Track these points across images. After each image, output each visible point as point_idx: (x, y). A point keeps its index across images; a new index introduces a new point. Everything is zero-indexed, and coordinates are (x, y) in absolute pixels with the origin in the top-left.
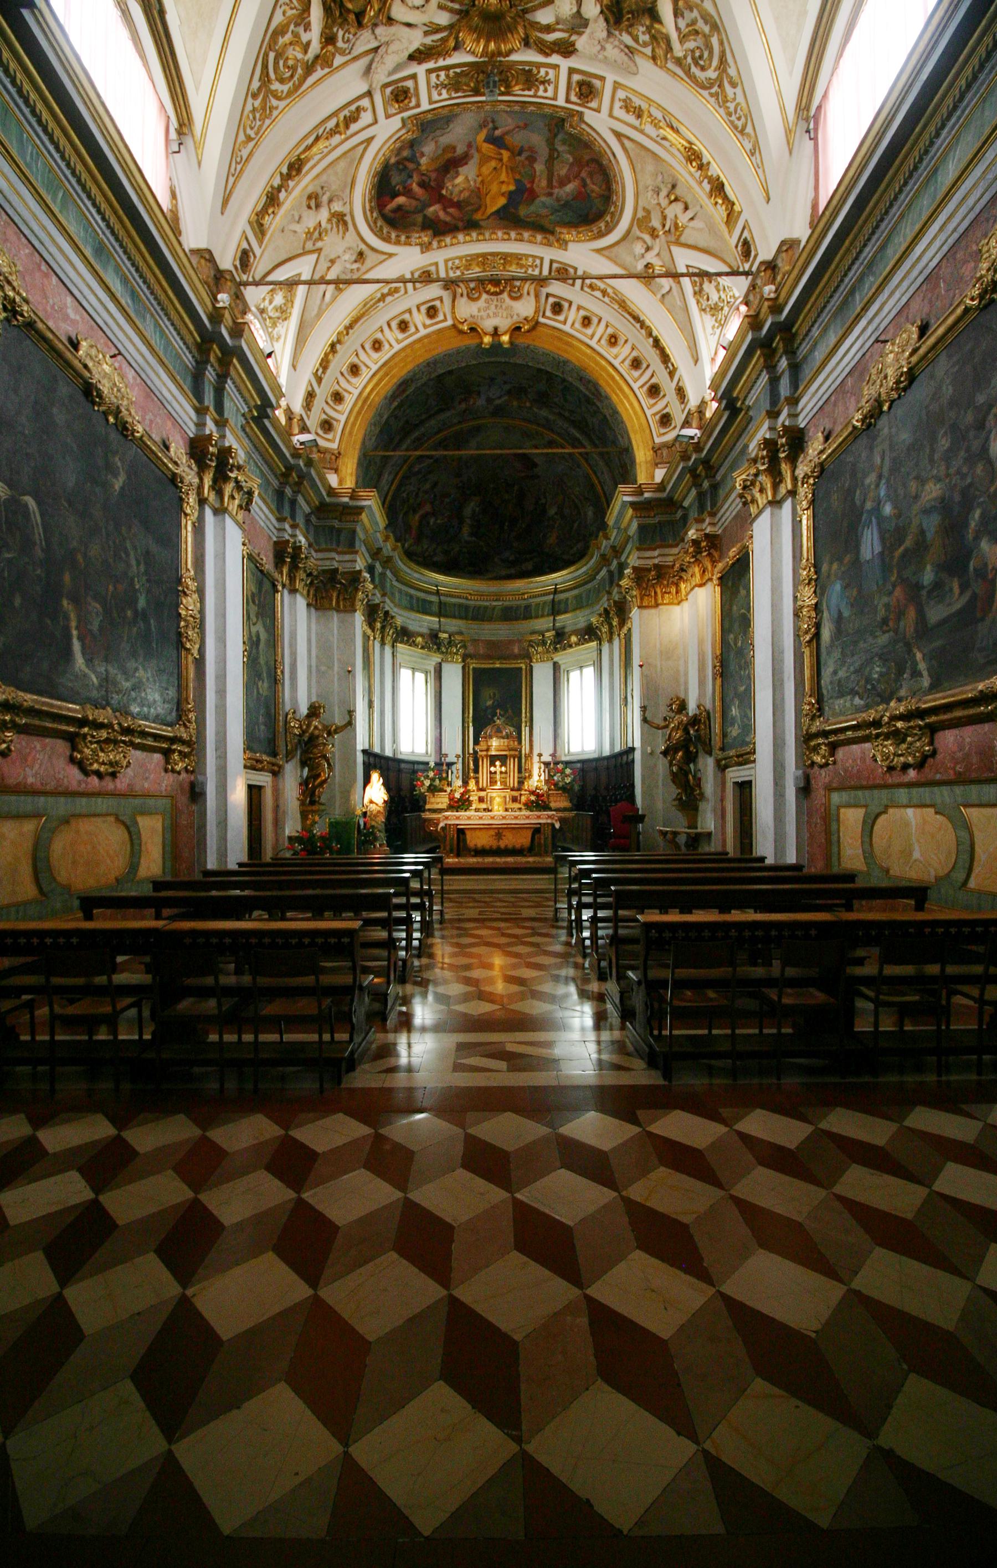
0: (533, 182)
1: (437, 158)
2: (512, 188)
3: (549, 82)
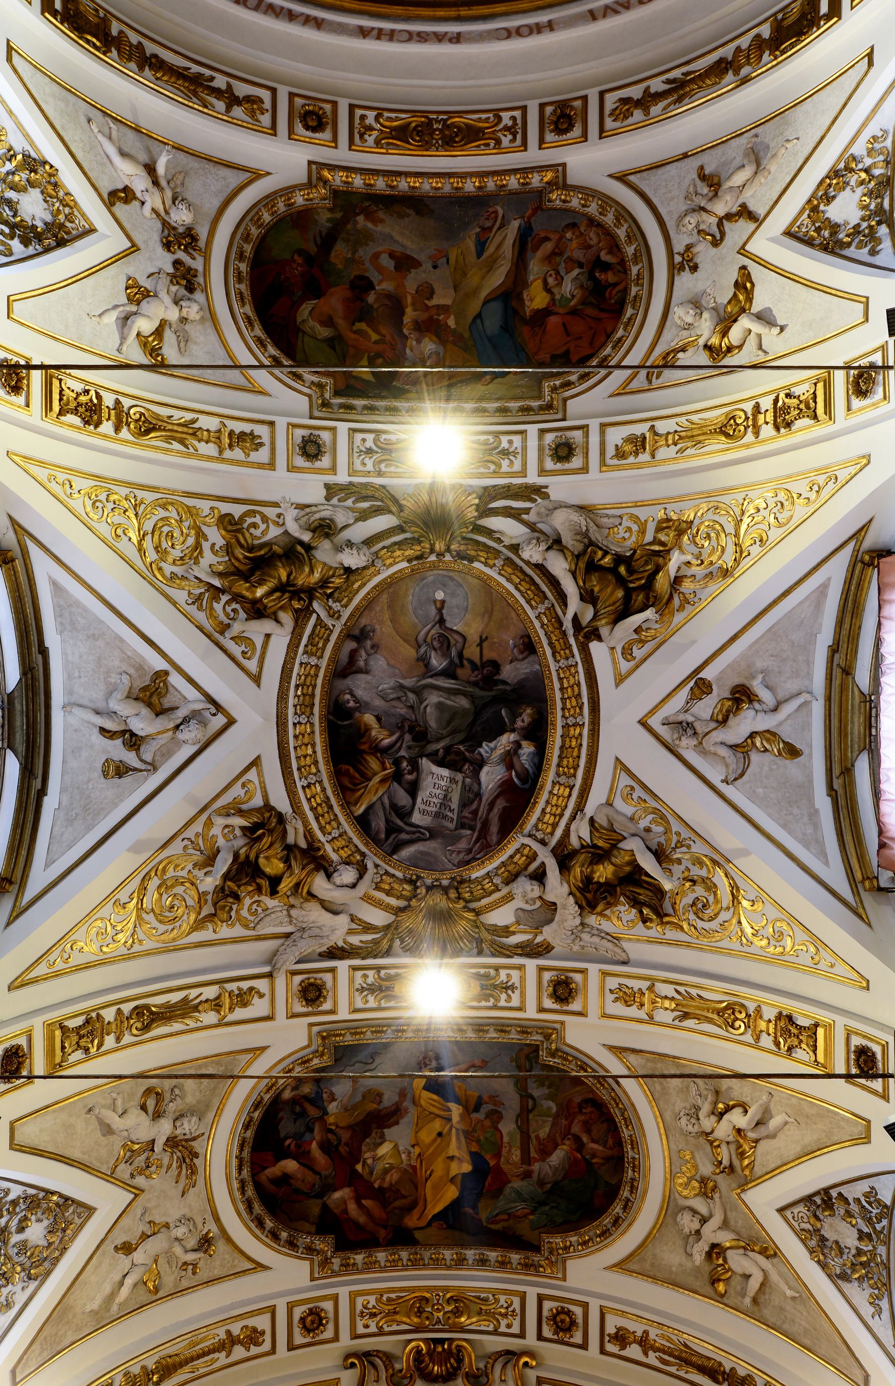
0: (498, 1155)
1: (354, 1107)
2: (467, 1168)
3: (512, 988)
